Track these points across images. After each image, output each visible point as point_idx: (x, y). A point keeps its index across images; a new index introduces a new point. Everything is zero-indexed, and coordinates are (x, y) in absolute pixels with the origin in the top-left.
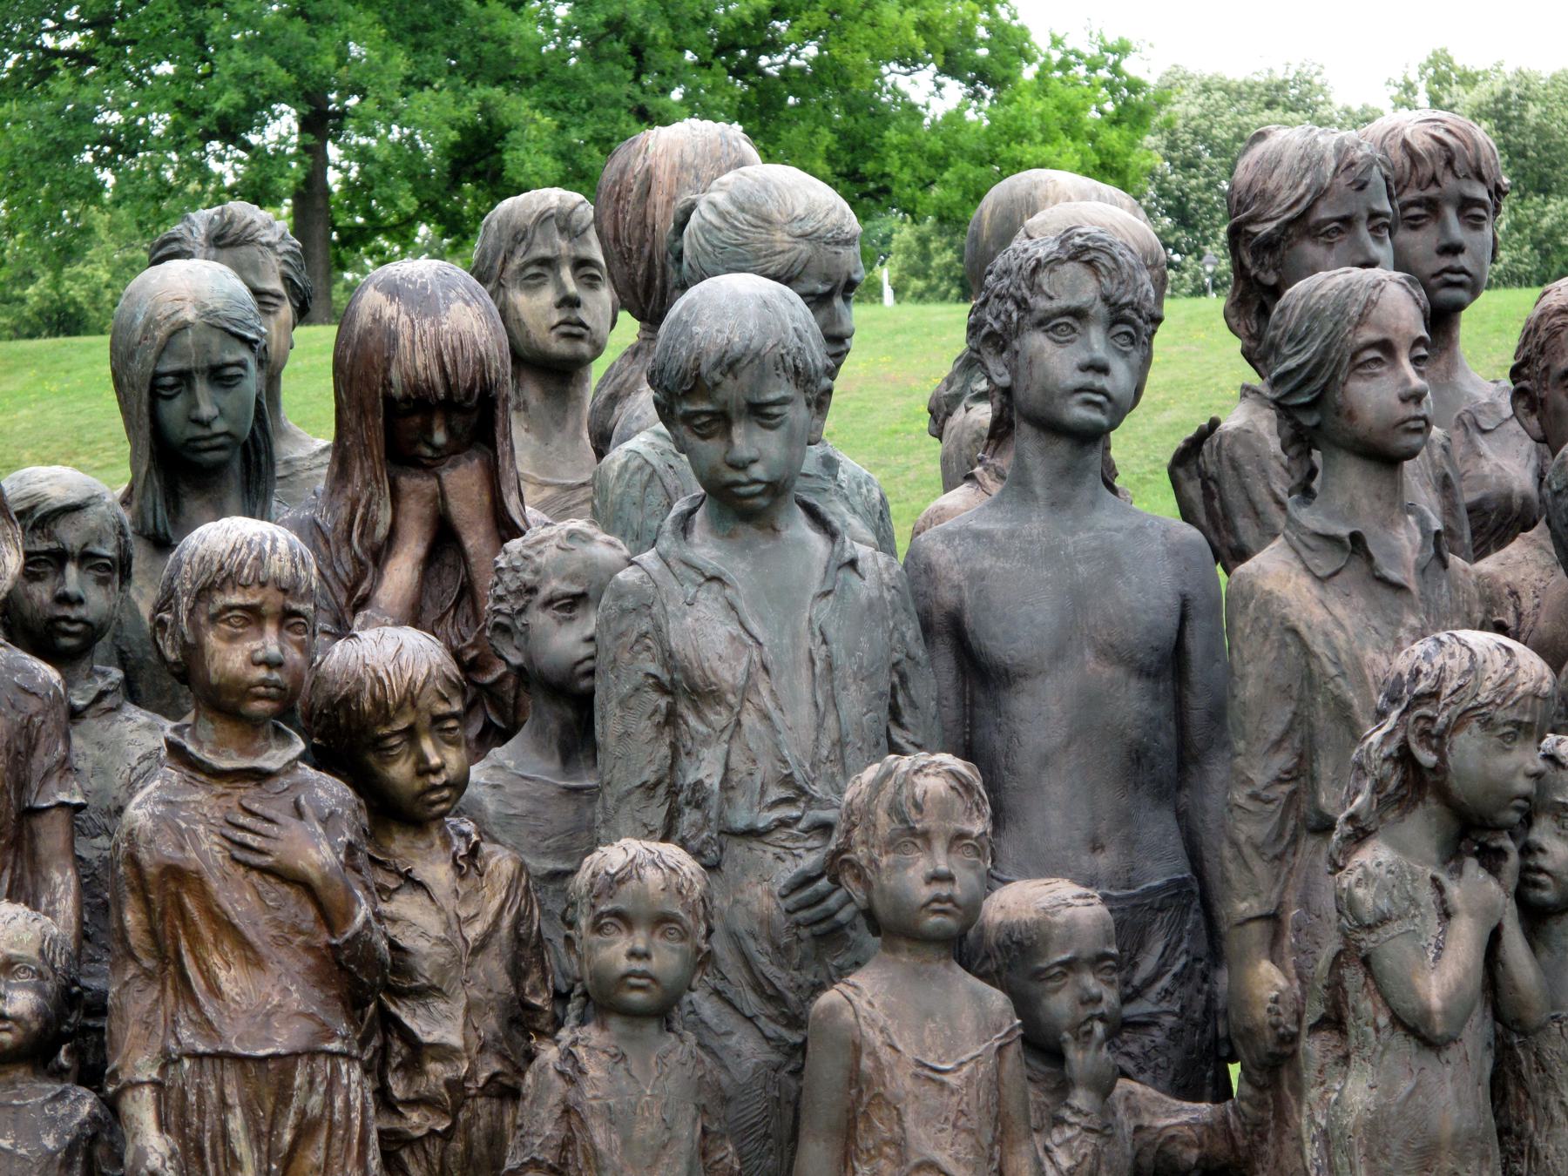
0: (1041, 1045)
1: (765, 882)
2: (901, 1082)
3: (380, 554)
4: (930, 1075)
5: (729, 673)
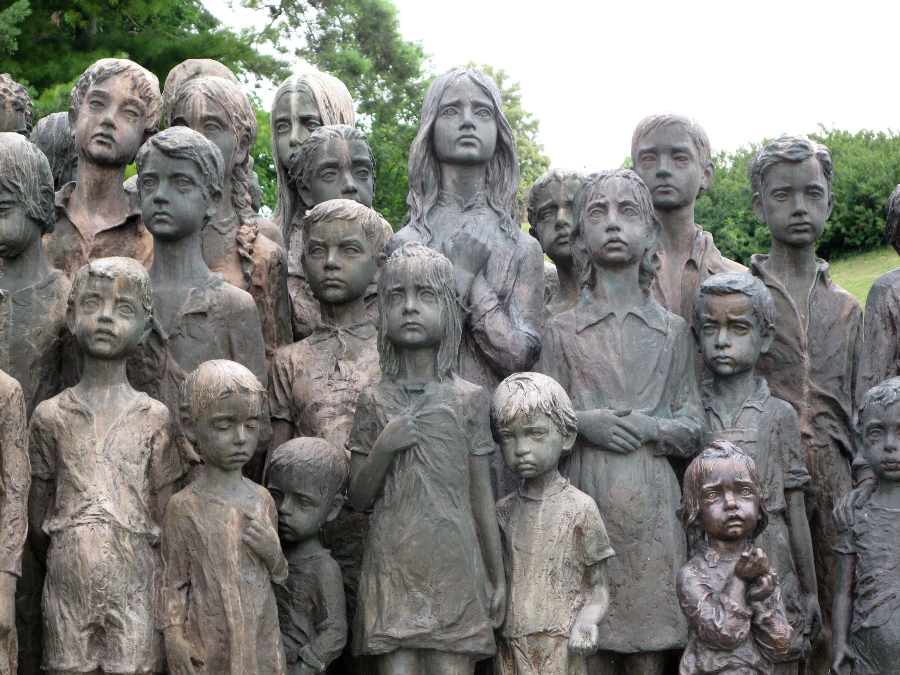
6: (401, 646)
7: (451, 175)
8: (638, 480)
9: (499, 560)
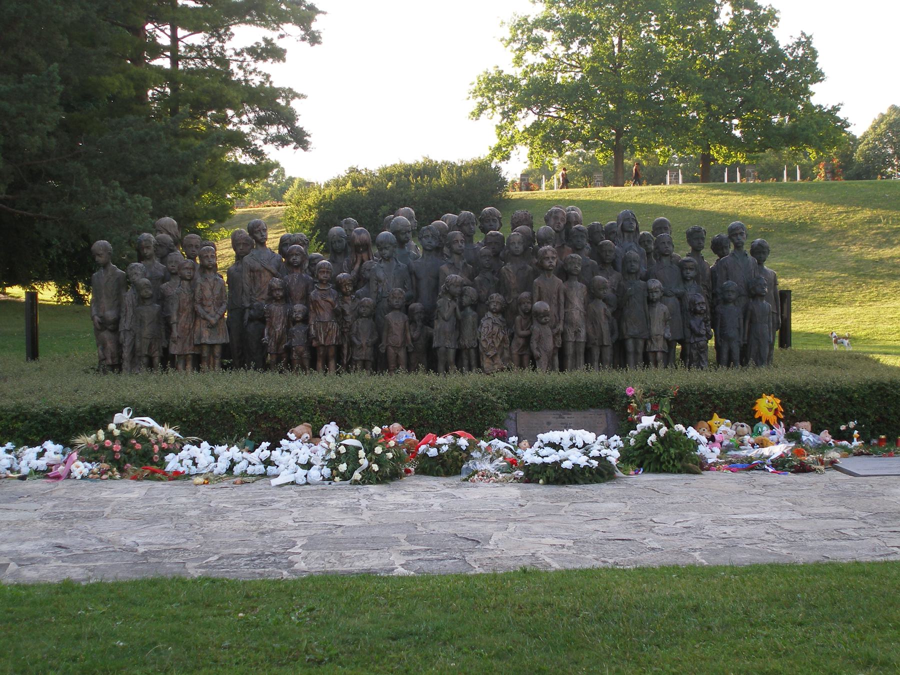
0: (412, 321)
1: (385, 304)
2: (393, 325)
3: (354, 264)
4: (396, 324)
5: (382, 278)
6: (632, 337)
7: (626, 235)
8: (673, 301)
9: (648, 321)
